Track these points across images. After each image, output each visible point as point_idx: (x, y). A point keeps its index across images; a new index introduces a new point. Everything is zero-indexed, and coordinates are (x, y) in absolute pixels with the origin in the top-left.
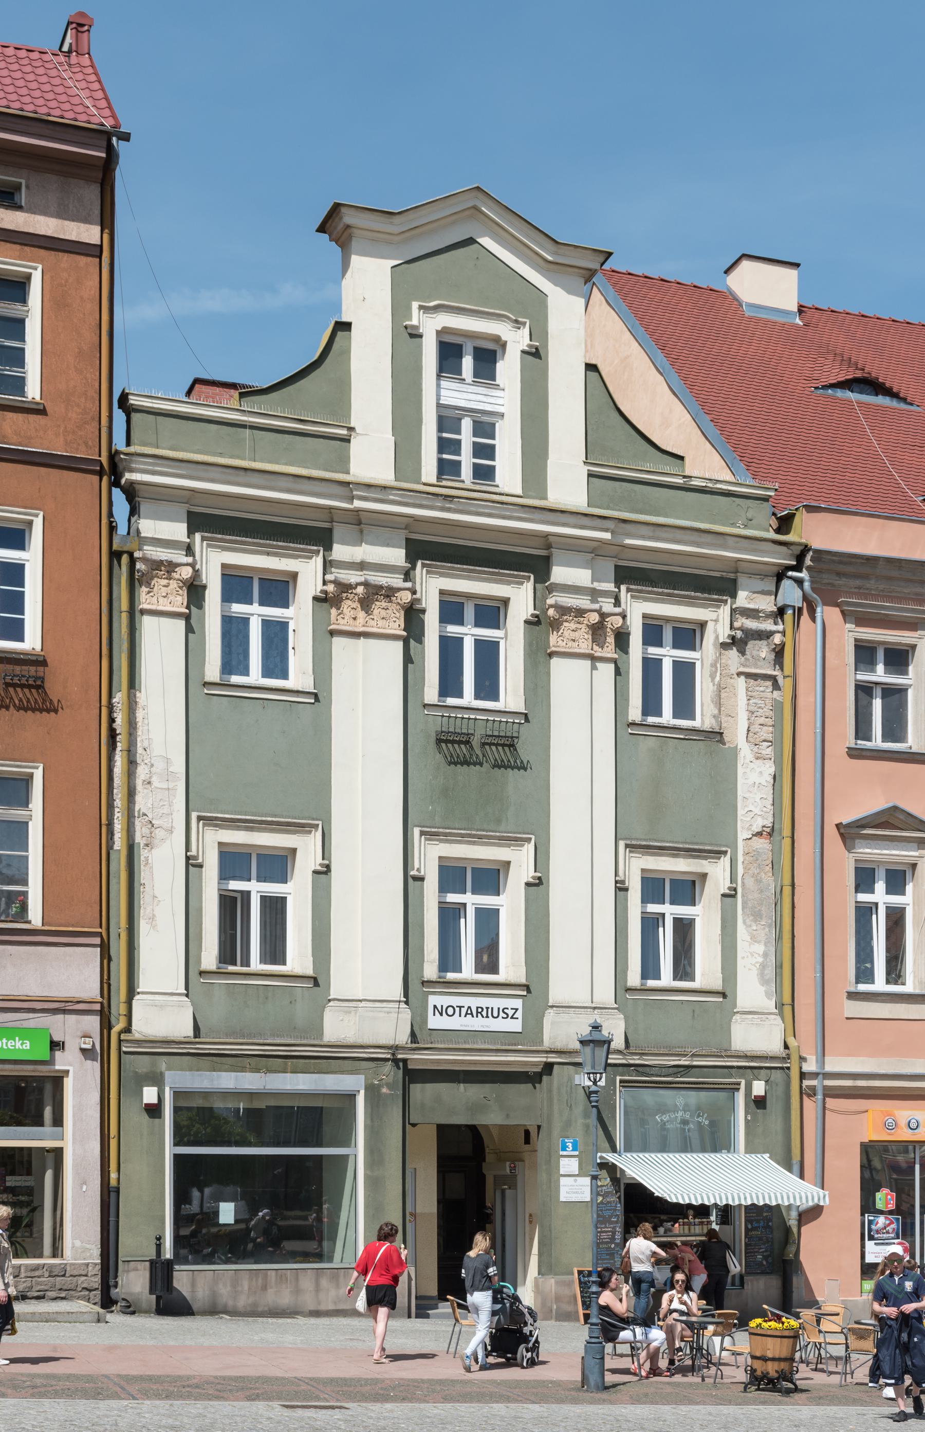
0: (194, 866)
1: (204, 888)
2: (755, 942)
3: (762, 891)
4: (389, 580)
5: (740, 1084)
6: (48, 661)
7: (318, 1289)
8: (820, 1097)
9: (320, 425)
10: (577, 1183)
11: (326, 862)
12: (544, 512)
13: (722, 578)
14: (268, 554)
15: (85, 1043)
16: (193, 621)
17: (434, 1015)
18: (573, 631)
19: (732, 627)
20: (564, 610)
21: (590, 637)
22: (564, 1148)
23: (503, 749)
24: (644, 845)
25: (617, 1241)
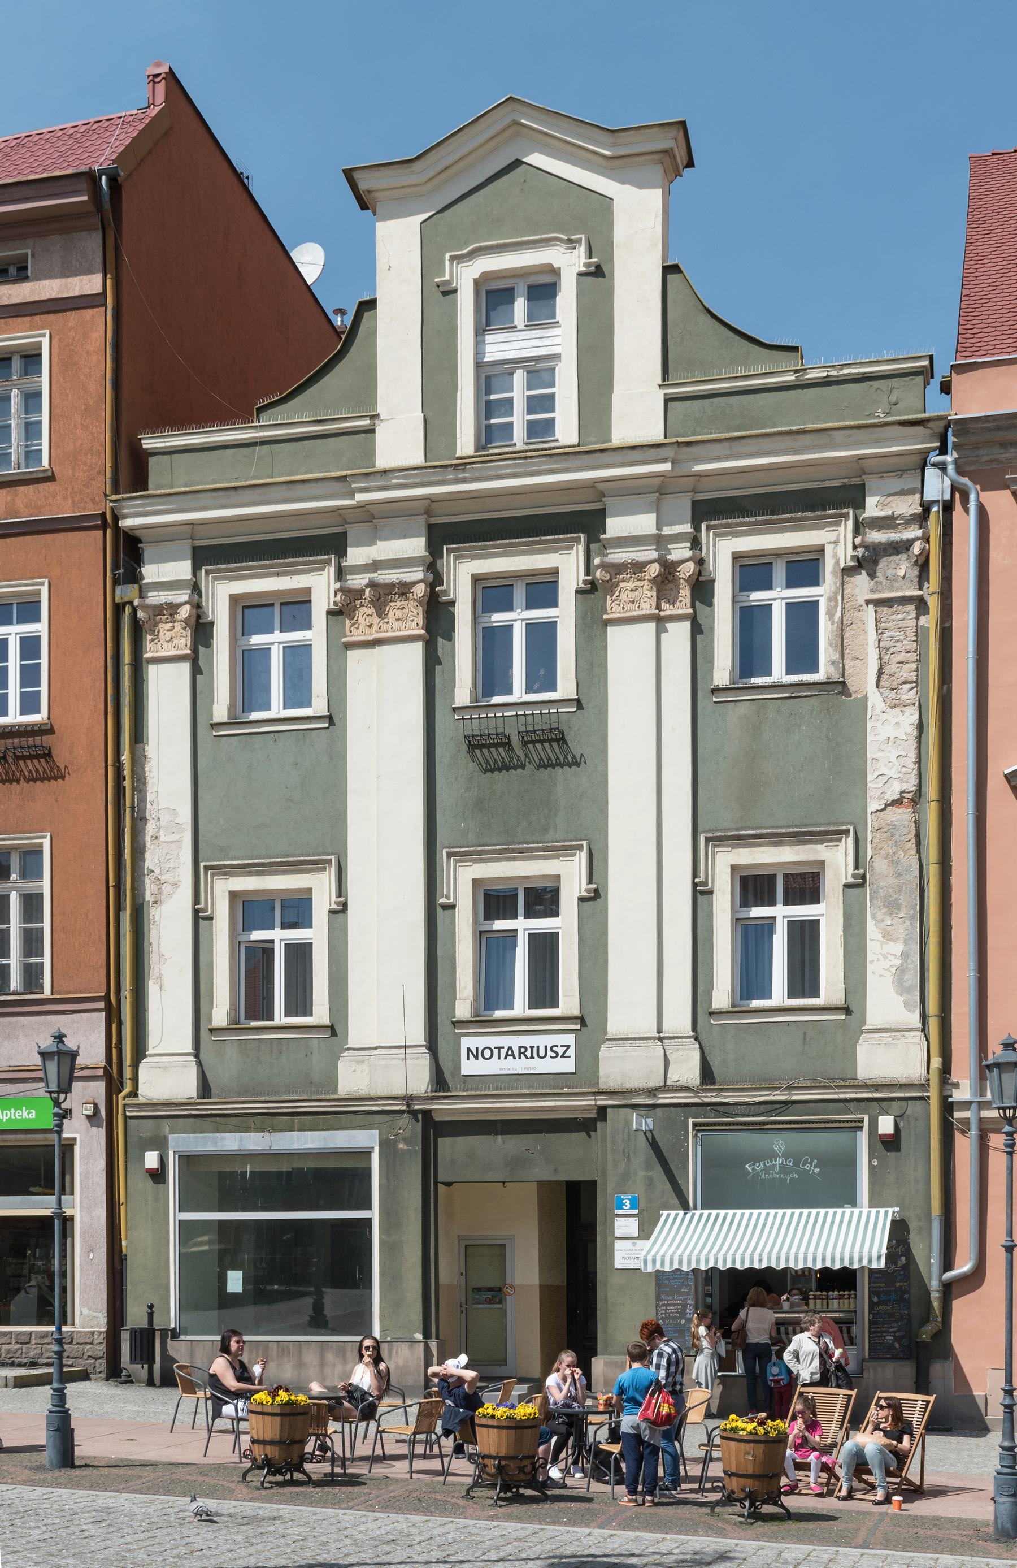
1: (214, 941)
2: (891, 940)
3: (900, 875)
4: (402, 575)
5: (863, 1121)
7: (322, 1363)
8: (974, 1132)
9: (339, 422)
11: (342, 899)
12: (578, 456)
13: (844, 486)
14: (278, 574)
16: (201, 663)
17: (468, 1059)
19: (855, 547)
20: (618, 569)
21: (654, 594)
23: (551, 745)
24: (732, 836)
25: (689, 1316)
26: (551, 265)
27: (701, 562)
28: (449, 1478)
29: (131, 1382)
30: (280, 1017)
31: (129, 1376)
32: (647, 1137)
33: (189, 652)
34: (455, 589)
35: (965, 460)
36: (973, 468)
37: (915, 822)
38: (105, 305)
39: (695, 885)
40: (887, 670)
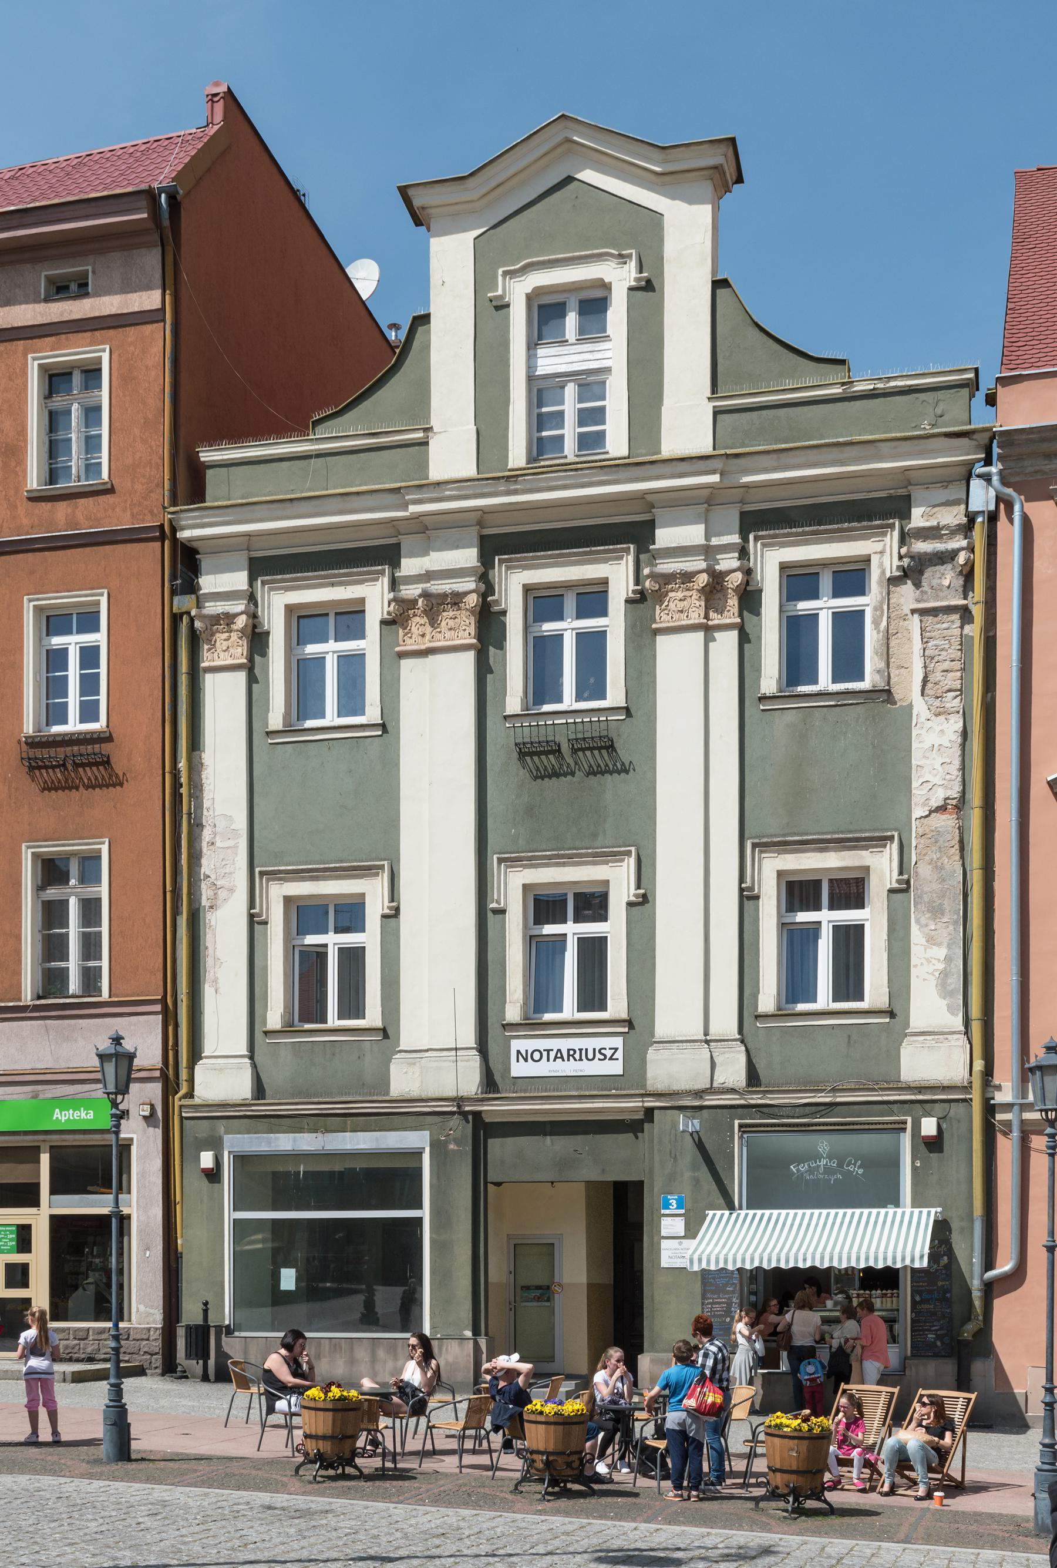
0: (259, 923)
2: (934, 945)
3: (944, 880)
4: (454, 585)
5: (906, 1123)
6: (114, 736)
7: (374, 1360)
8: (1016, 1134)
10: (682, 1247)
13: (890, 498)
14: (333, 585)
15: (143, 1110)
16: (257, 671)
17: (518, 1061)
18: (680, 600)
19: (901, 558)
20: (667, 579)
21: (703, 604)
22: (667, 1206)
23: (600, 753)
24: (779, 842)
26: (602, 280)
27: (748, 572)
28: (498, 1473)
29: (187, 1377)
30: (333, 1020)
31: (185, 1372)
32: (693, 1138)
33: (245, 661)
34: (506, 599)
35: (1010, 471)
36: (1018, 479)
37: (959, 828)
38: (164, 321)
39: (741, 890)
40: (931, 678)
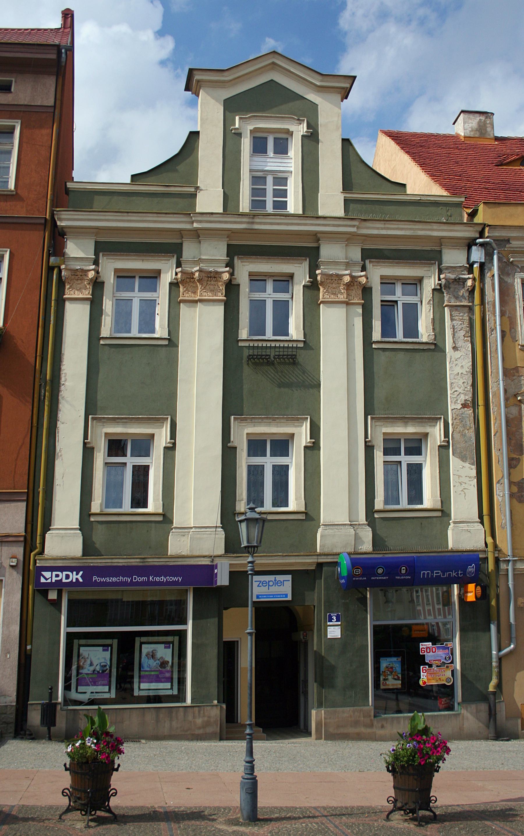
39: (366, 442)
